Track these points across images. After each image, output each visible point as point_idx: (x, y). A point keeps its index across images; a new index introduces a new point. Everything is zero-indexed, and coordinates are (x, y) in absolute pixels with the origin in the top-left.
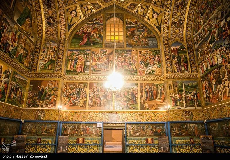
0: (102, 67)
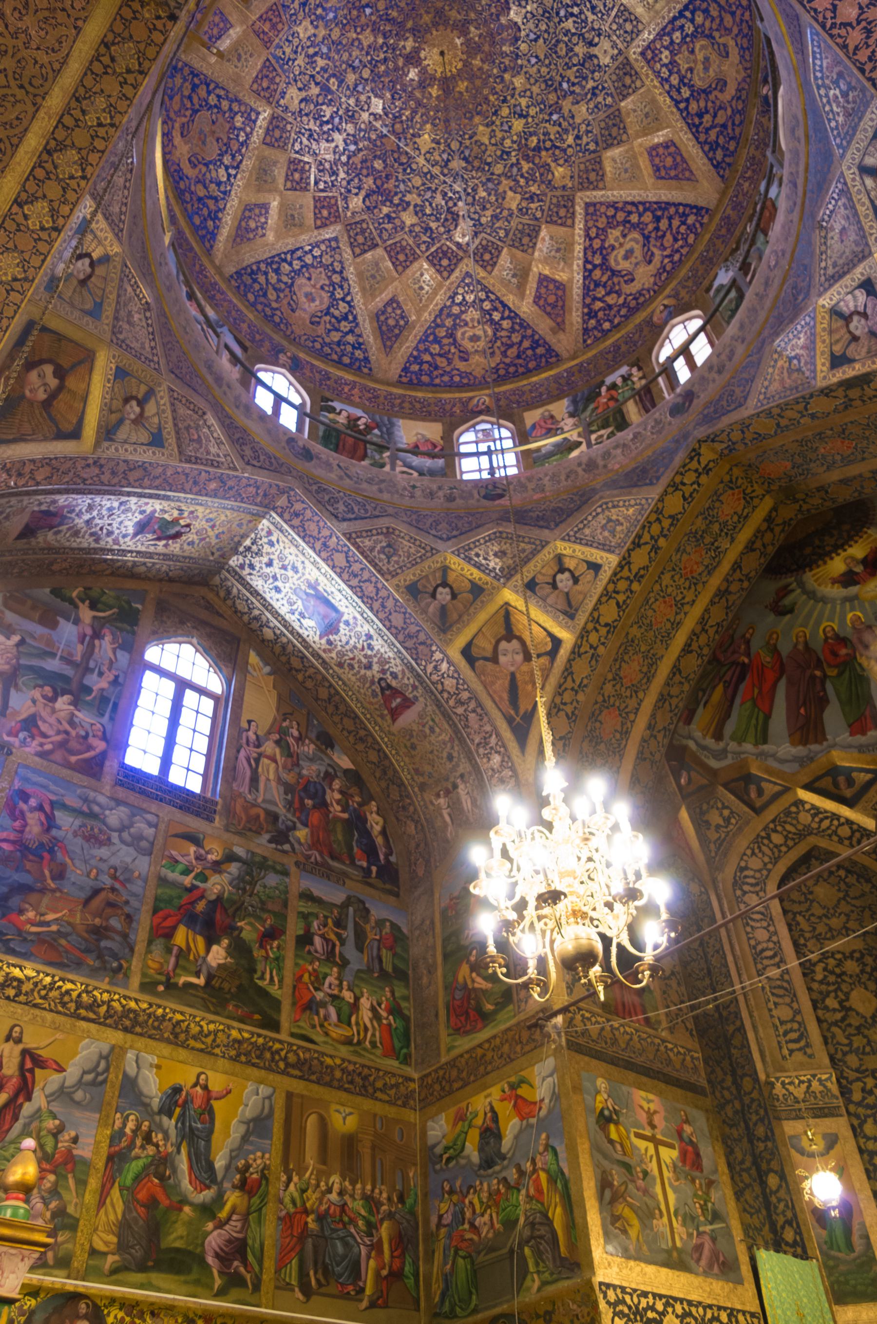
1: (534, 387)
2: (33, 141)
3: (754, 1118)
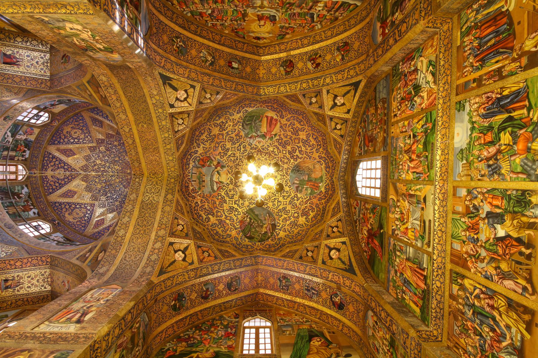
0: (418, 214)
1: (46, 135)
2: (138, 141)
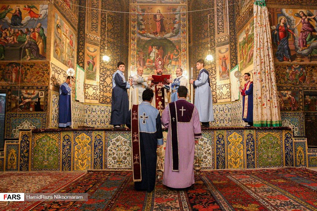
3: (81, 40)
